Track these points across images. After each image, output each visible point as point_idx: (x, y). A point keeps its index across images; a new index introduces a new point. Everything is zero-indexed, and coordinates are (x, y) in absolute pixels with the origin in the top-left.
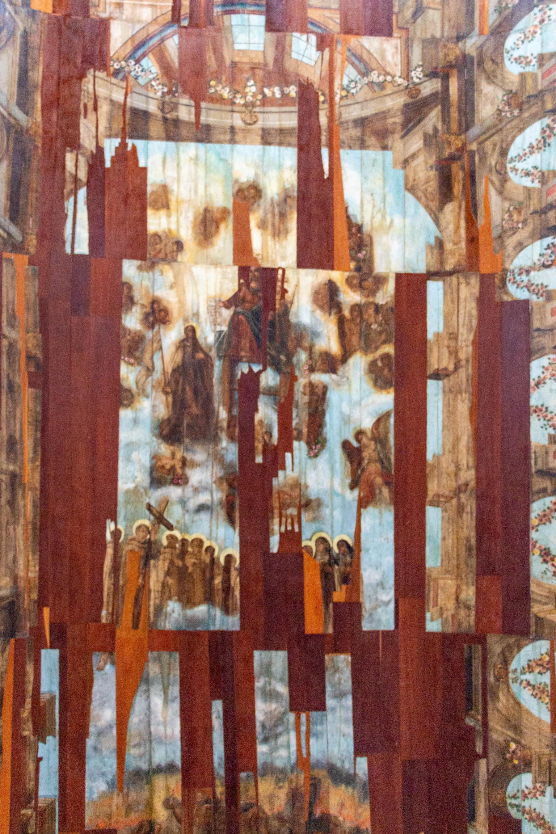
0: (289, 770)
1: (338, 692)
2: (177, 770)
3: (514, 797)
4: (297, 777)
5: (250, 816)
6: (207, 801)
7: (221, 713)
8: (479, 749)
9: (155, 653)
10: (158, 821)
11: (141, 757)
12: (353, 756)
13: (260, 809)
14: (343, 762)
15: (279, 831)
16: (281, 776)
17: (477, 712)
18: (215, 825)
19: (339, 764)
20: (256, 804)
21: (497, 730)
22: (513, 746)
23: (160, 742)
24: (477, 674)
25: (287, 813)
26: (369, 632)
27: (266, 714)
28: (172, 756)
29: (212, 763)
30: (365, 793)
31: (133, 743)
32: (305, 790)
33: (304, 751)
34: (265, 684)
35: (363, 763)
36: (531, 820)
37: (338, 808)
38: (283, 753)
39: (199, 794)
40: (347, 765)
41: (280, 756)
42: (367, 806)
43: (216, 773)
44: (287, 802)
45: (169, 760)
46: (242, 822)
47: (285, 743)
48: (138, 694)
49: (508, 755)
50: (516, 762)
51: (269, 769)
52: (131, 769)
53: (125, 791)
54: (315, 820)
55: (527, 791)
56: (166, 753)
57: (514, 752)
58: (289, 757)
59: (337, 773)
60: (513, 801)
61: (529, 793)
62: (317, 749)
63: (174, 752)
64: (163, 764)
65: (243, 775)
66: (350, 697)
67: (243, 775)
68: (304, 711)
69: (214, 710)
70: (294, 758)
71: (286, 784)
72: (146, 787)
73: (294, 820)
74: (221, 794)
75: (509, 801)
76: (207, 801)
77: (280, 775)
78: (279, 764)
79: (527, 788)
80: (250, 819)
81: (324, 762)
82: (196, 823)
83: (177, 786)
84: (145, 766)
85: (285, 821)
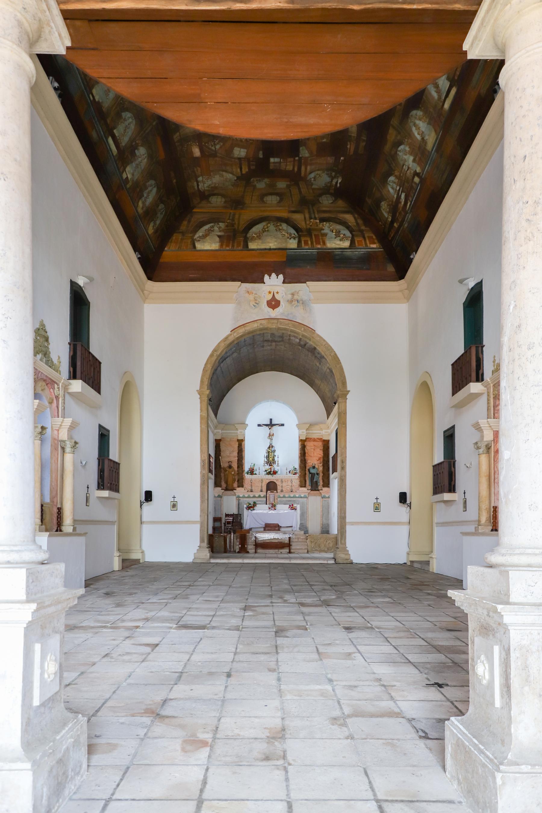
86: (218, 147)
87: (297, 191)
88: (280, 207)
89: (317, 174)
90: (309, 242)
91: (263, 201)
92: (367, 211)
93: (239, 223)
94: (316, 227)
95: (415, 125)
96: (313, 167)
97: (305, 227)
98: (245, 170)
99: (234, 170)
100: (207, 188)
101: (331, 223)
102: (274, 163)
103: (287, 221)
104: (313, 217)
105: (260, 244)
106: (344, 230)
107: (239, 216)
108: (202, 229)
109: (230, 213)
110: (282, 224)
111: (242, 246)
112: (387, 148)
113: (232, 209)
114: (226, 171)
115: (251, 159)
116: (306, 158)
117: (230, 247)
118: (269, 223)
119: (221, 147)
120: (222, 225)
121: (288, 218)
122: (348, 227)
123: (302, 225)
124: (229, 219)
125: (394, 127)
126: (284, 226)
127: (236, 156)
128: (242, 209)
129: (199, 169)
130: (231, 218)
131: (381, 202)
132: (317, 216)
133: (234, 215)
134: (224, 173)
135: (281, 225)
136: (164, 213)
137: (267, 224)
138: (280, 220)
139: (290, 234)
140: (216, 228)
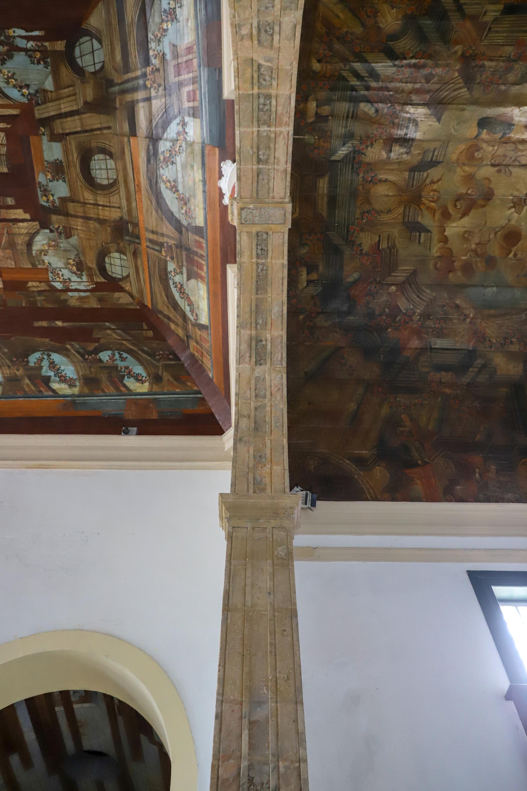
87: (69, 119)
88: (123, 153)
89: (8, 83)
100: (85, 278)
108: (179, 303)
109: (147, 247)
113: (139, 244)
117: (203, 262)
120: (171, 266)
128: (136, 225)
129: (30, 284)
130: (157, 248)
133: (151, 241)
134: (36, 248)
136: (125, 355)
140: (177, 278)
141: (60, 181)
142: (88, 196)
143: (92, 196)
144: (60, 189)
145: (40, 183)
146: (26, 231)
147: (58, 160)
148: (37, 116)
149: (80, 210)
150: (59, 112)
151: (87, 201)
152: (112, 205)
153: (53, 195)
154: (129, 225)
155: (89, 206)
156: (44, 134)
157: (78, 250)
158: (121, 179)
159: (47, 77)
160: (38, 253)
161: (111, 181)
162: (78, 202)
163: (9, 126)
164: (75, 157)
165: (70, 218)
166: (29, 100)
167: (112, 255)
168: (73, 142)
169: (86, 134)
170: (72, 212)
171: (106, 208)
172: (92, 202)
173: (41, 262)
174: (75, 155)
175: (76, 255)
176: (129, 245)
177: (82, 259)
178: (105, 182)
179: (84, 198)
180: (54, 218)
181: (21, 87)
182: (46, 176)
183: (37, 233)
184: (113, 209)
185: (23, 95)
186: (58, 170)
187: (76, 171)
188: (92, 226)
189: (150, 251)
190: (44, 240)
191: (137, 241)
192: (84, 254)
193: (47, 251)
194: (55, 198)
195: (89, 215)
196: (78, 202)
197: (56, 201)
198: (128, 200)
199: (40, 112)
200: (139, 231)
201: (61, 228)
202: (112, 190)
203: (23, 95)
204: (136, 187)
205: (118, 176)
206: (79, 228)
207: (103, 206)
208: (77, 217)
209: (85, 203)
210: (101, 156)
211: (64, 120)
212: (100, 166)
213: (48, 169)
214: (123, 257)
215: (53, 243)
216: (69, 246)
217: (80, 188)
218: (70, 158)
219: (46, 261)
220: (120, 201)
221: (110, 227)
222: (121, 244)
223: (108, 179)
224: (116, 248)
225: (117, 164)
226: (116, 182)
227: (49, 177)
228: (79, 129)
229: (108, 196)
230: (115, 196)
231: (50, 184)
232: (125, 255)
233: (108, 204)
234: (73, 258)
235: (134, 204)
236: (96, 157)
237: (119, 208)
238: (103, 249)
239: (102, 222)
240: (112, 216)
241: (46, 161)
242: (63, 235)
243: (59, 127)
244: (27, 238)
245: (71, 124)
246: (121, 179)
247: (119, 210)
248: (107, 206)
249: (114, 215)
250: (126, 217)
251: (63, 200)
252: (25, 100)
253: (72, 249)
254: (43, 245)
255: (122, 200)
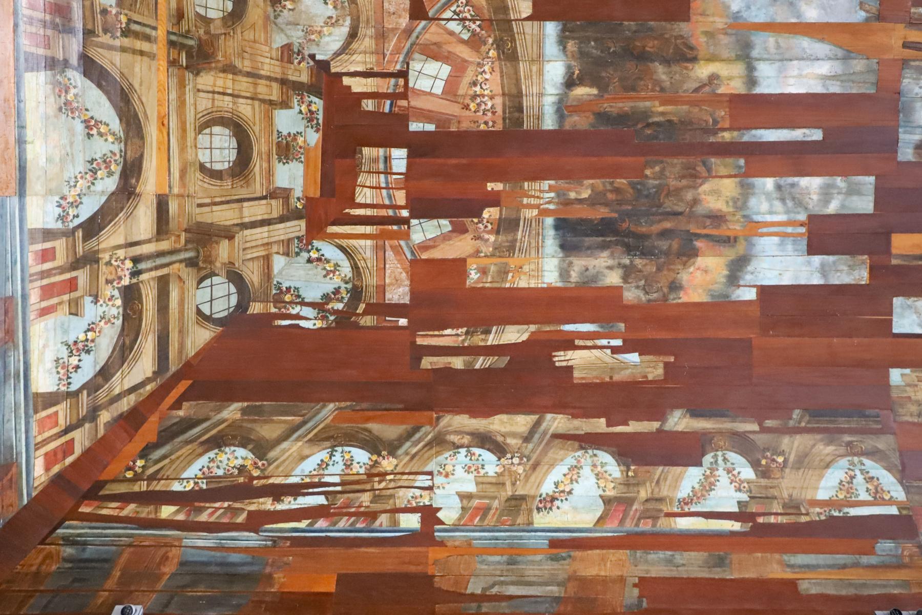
0: (745, 213)
1: (827, 268)
2: (750, 89)
3: (725, 460)
4: (738, 221)
5: (698, 169)
6: (715, 122)
7: (809, 139)
8: (769, 423)
9: (876, 67)
10: (697, 66)
11: (766, 49)
12: (759, 284)
13: (706, 179)
14: (752, 273)
15: (682, 200)
16: (739, 203)
17: (808, 422)
18: (690, 130)
19: (749, 268)
20: (710, 174)
21: (793, 443)
22: (780, 459)
23: (780, 71)
24: (848, 422)
25: (700, 210)
26: (891, 304)
27: (807, 188)
28: (765, 83)
29: (756, 128)
30: (719, 296)
31: (780, 40)
32: (723, 231)
33: (765, 230)
34: (838, 187)
35: (750, 295)
36: (706, 477)
37: (703, 266)
38: (765, 206)
39: (723, 113)
40: (748, 277)
41: (761, 203)
42: (705, 298)
43: (745, 132)
44: (711, 211)
45: (761, 80)
46: (692, 159)
47: (774, 209)
48: (833, 47)
49: (768, 454)
50: (764, 462)
51: (747, 191)
52: (753, 38)
53: (729, 31)
54: (692, 240)
55: (735, 472)
56: (768, 77)
57: (774, 460)
58: (758, 213)
59: (741, 267)
60: (720, 459)
61: (733, 475)
62: (767, 244)
63: (769, 86)
64: (756, 74)
65: (742, 162)
66: (821, 282)
67: (742, 162)
68: (810, 232)
69: (814, 131)
70: (759, 218)
71: (731, 210)
72: (733, 55)
73: (692, 216)
74: (723, 137)
75: (720, 453)
76: (715, 122)
77: (741, 203)
78: (752, 202)
79: (739, 473)
80: (694, 169)
81: (753, 252)
82: (691, 109)
83: (732, 89)
84: (755, 53)
85: (692, 207)
86: (454, 26)
87: (259, 218)
88: (183, 173)
90: (47, 266)
91: (208, 124)
92: (181, 413)
93: (111, 48)
94: (102, 280)
95: (576, 468)
96: (368, 254)
97: (102, 246)
98: (358, 85)
99: (358, 58)
101: (119, 322)
102: (387, 159)
103: (126, 192)
104: (142, 266)
105: (42, 109)
106: (96, 362)
107: (142, 53)
110: (116, 177)
111: (33, 50)
112: (463, 421)
114: (353, 35)
115: (403, 103)
116: (407, 236)
118: (119, 140)
119: (451, 33)
121: (139, 195)
122: (105, 373)
123: (112, 238)
124: (130, 21)
125: (538, 424)
126: (109, 184)
127: (415, 66)
128: (173, 63)
131: (244, 446)
132: (144, 277)
134: (343, 31)
135: (110, 174)
137: (114, 134)
138: (131, 170)
139: (75, 204)
141: (285, 133)
142: (246, 109)
143: (239, 110)
144: (287, 121)
145: (317, 131)
146: (355, 56)
147: (284, 164)
148: (303, 223)
149: (263, 89)
150: (271, 227)
151: (249, 101)
152: (210, 95)
153: (301, 112)
154: (184, 64)
155: (248, 95)
156: (298, 199)
157: (275, 24)
158: (191, 134)
159: (280, 272)
160: (341, 22)
161: (207, 131)
162: (263, 101)
163: (347, 211)
164: (257, 166)
165: (279, 76)
166: (311, 244)
167: (221, 15)
168: (258, 188)
169: (237, 197)
170: (275, 85)
171: (221, 90)
172: (241, 100)
173: (339, 7)
174: (257, 169)
175: (279, 15)
176: (188, 31)
177: (270, 9)
178: (217, 129)
179: (253, 106)
180: (304, 78)
181: (319, 260)
182: (305, 141)
183: (337, 54)
184: (211, 89)
185: (318, 250)
186: (286, 149)
187: (260, 146)
188: (247, 63)
189: (152, 22)
190: (327, 43)
191: (174, 38)
192: (267, 18)
193: (326, 23)
194: (297, 108)
195: (250, 80)
196: (263, 101)
197: (296, 103)
198: (182, 103)
199: (298, 228)
200: (169, 53)
201: (296, 61)
202: (207, 118)
203: (318, 250)
204: (166, 122)
205: (195, 139)
206: (268, 61)
207: (224, 94)
208: (269, 78)
209: (252, 99)
210: (218, 167)
211: (266, 217)
212: (221, 153)
213: (302, 151)
214: (202, 11)
215: (313, 37)
216: (288, 32)
217: (257, 122)
218: (265, 165)
219: (330, 7)
220: (196, 101)
221: (219, 61)
222: (202, 32)
223: (211, 134)
224: (211, 25)
225: (194, 155)
226: (200, 129)
227: (300, 140)
228: (245, 204)
229: (214, 109)
230: (204, 108)
231: (301, 129)
232: (198, 15)
233: (216, 96)
234: (285, 11)
235: (173, 95)
236: (226, 166)
237: (199, 90)
238: (233, 24)
239: (229, 69)
240: (212, 78)
241: (301, 162)
242: (296, 50)
243: (275, 208)
244: (354, 46)
245: (255, 211)
246: (191, 134)
247: (200, 87)
248: (219, 93)
249: (206, 80)
250: (189, 76)
251: (285, 104)
252: (316, 243)
253: (283, 26)
254: (330, 34)
255: (192, 101)
